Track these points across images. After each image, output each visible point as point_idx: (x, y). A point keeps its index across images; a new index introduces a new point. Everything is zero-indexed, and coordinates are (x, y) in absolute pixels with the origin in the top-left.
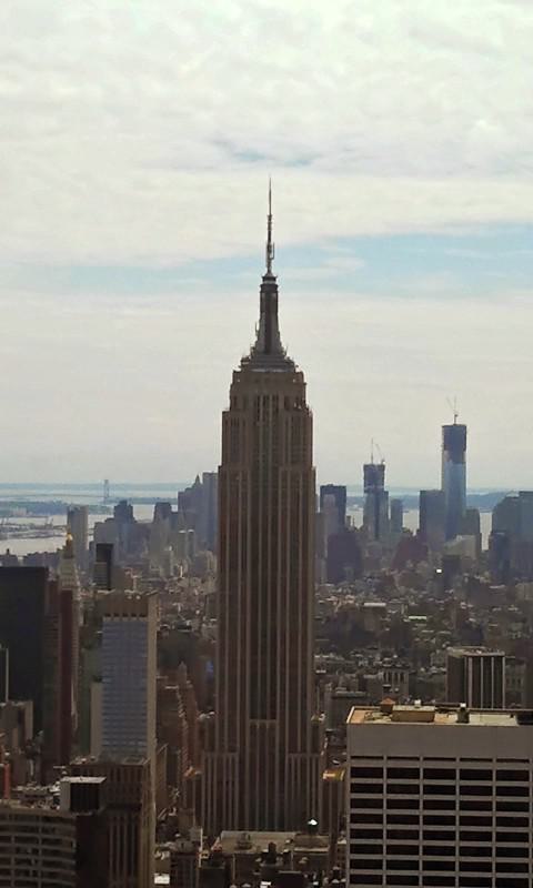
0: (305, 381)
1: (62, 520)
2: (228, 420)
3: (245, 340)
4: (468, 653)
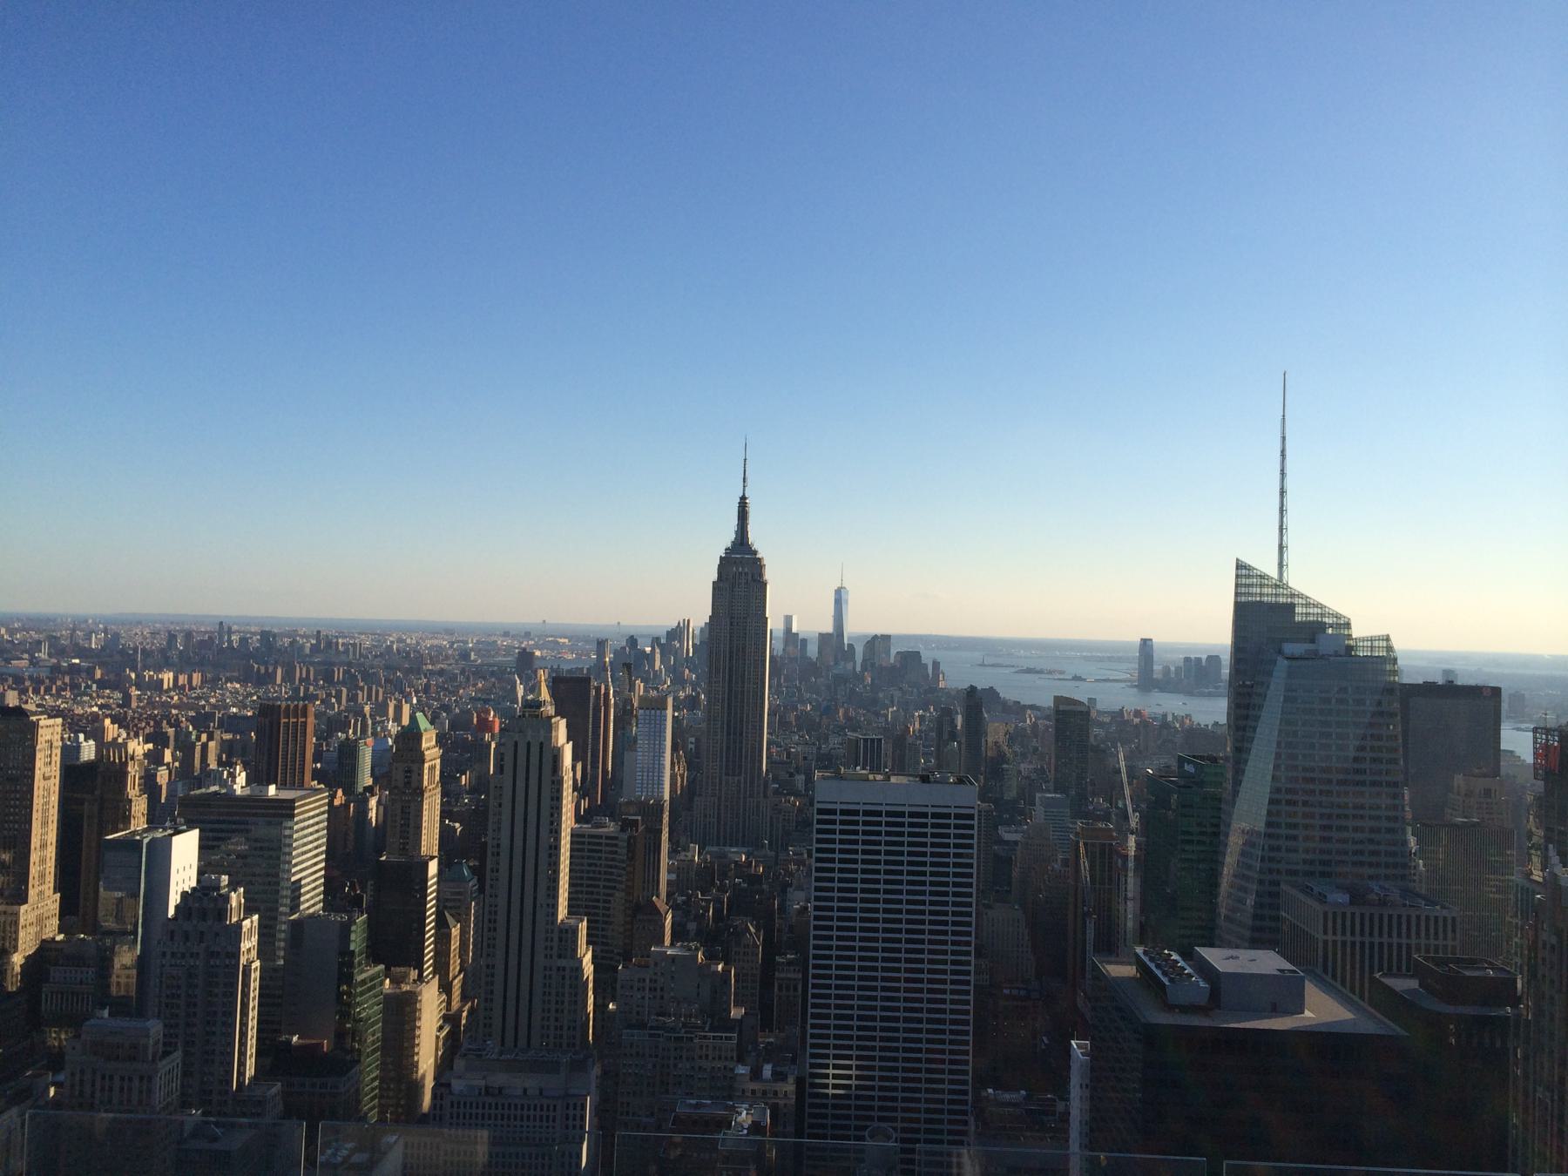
0: (765, 562)
1: (594, 647)
2: (717, 587)
3: (728, 537)
4: (861, 737)
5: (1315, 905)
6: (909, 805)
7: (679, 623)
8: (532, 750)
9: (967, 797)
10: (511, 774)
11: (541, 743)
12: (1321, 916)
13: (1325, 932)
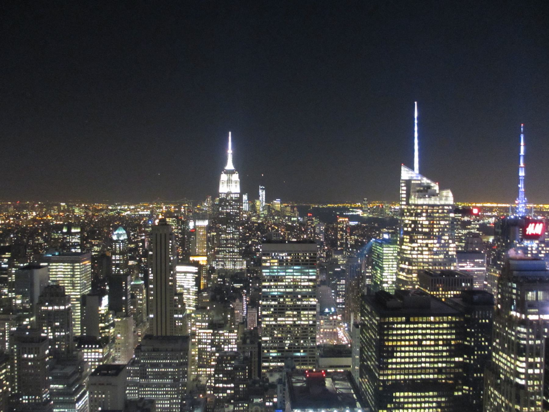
11: (165, 235)
13: (432, 286)
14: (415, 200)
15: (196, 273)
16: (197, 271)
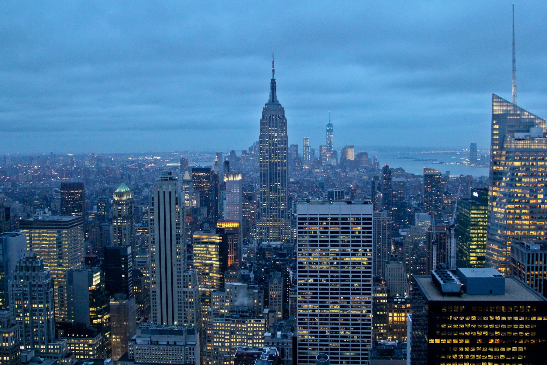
5: (524, 250)
6: (341, 215)
7: (254, 143)
8: (166, 194)
9: (368, 210)
10: (157, 206)
11: (170, 192)
12: (527, 256)
14: (511, 142)
15: (220, 244)
16: (221, 241)
